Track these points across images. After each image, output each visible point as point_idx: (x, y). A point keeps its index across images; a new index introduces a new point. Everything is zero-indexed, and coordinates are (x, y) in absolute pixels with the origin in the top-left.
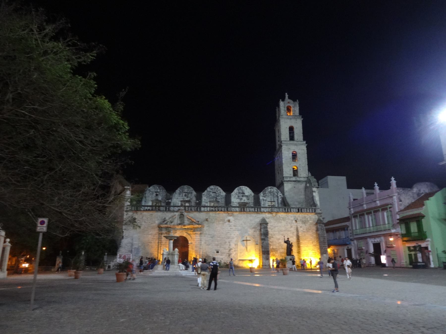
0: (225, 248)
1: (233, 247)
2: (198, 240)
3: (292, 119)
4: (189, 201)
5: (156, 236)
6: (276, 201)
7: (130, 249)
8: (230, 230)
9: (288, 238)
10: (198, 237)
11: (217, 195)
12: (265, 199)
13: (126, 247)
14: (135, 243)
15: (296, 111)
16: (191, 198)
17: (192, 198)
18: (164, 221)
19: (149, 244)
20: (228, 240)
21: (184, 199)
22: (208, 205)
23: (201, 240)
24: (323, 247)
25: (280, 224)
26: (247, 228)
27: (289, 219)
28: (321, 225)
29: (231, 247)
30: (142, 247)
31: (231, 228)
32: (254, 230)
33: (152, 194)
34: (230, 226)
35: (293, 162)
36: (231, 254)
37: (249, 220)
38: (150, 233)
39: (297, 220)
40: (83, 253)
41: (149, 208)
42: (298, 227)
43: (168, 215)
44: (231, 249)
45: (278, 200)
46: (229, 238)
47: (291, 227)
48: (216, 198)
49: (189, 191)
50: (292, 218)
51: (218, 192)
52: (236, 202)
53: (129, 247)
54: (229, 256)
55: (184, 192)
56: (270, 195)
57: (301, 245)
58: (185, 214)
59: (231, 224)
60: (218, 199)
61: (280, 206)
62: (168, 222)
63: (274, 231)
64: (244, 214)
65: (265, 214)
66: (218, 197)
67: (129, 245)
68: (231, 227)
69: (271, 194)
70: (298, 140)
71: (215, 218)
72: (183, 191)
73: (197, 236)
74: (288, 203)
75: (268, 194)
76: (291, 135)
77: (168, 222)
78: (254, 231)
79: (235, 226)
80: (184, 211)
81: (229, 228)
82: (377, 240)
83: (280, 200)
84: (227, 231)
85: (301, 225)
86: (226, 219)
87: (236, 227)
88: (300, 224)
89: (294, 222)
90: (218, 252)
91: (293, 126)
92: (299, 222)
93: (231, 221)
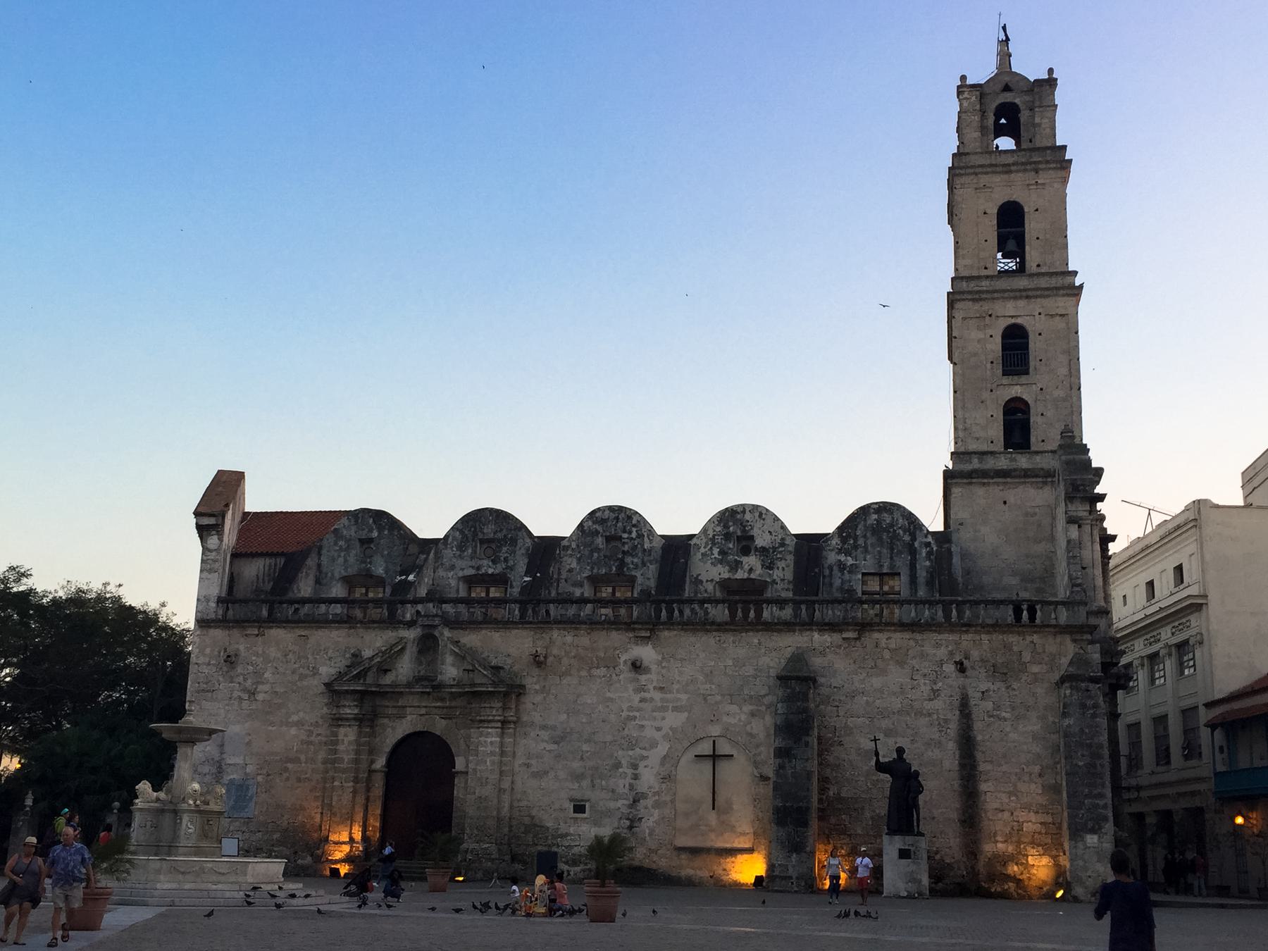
1: (650, 787)
2: (492, 753)
4: (501, 580)
5: (320, 731)
9: (900, 751)
10: (493, 739)
11: (626, 548)
12: (850, 561)
14: (230, 762)
15: (1039, 125)
16: (510, 564)
17: (514, 565)
19: (290, 766)
20: (631, 753)
21: (478, 568)
22: (583, 593)
23: (503, 753)
25: (877, 682)
26: (719, 698)
27: (923, 656)
29: (642, 786)
30: (260, 778)
32: (751, 707)
33: (348, 549)
34: (642, 689)
35: (1005, 380)
37: (730, 663)
38: (295, 718)
39: (966, 662)
40: (29, 802)
41: (337, 609)
42: (970, 692)
47: (935, 694)
48: (622, 564)
49: (504, 532)
50: (942, 653)
51: (630, 533)
52: (712, 580)
55: (480, 536)
57: (983, 787)
58: (442, 634)
60: (631, 566)
61: (922, 593)
62: (369, 669)
65: (808, 633)
66: (628, 559)
67: (206, 769)
69: (880, 540)
70: (1043, 270)
72: (475, 534)
75: (865, 536)
77: (369, 669)
78: (753, 714)
81: (637, 698)
83: (924, 564)
84: (624, 714)
85: (983, 687)
87: (668, 696)
88: (979, 683)
89: (950, 668)
90: (579, 809)
91: (1017, 200)
92: (973, 668)
93: (646, 663)
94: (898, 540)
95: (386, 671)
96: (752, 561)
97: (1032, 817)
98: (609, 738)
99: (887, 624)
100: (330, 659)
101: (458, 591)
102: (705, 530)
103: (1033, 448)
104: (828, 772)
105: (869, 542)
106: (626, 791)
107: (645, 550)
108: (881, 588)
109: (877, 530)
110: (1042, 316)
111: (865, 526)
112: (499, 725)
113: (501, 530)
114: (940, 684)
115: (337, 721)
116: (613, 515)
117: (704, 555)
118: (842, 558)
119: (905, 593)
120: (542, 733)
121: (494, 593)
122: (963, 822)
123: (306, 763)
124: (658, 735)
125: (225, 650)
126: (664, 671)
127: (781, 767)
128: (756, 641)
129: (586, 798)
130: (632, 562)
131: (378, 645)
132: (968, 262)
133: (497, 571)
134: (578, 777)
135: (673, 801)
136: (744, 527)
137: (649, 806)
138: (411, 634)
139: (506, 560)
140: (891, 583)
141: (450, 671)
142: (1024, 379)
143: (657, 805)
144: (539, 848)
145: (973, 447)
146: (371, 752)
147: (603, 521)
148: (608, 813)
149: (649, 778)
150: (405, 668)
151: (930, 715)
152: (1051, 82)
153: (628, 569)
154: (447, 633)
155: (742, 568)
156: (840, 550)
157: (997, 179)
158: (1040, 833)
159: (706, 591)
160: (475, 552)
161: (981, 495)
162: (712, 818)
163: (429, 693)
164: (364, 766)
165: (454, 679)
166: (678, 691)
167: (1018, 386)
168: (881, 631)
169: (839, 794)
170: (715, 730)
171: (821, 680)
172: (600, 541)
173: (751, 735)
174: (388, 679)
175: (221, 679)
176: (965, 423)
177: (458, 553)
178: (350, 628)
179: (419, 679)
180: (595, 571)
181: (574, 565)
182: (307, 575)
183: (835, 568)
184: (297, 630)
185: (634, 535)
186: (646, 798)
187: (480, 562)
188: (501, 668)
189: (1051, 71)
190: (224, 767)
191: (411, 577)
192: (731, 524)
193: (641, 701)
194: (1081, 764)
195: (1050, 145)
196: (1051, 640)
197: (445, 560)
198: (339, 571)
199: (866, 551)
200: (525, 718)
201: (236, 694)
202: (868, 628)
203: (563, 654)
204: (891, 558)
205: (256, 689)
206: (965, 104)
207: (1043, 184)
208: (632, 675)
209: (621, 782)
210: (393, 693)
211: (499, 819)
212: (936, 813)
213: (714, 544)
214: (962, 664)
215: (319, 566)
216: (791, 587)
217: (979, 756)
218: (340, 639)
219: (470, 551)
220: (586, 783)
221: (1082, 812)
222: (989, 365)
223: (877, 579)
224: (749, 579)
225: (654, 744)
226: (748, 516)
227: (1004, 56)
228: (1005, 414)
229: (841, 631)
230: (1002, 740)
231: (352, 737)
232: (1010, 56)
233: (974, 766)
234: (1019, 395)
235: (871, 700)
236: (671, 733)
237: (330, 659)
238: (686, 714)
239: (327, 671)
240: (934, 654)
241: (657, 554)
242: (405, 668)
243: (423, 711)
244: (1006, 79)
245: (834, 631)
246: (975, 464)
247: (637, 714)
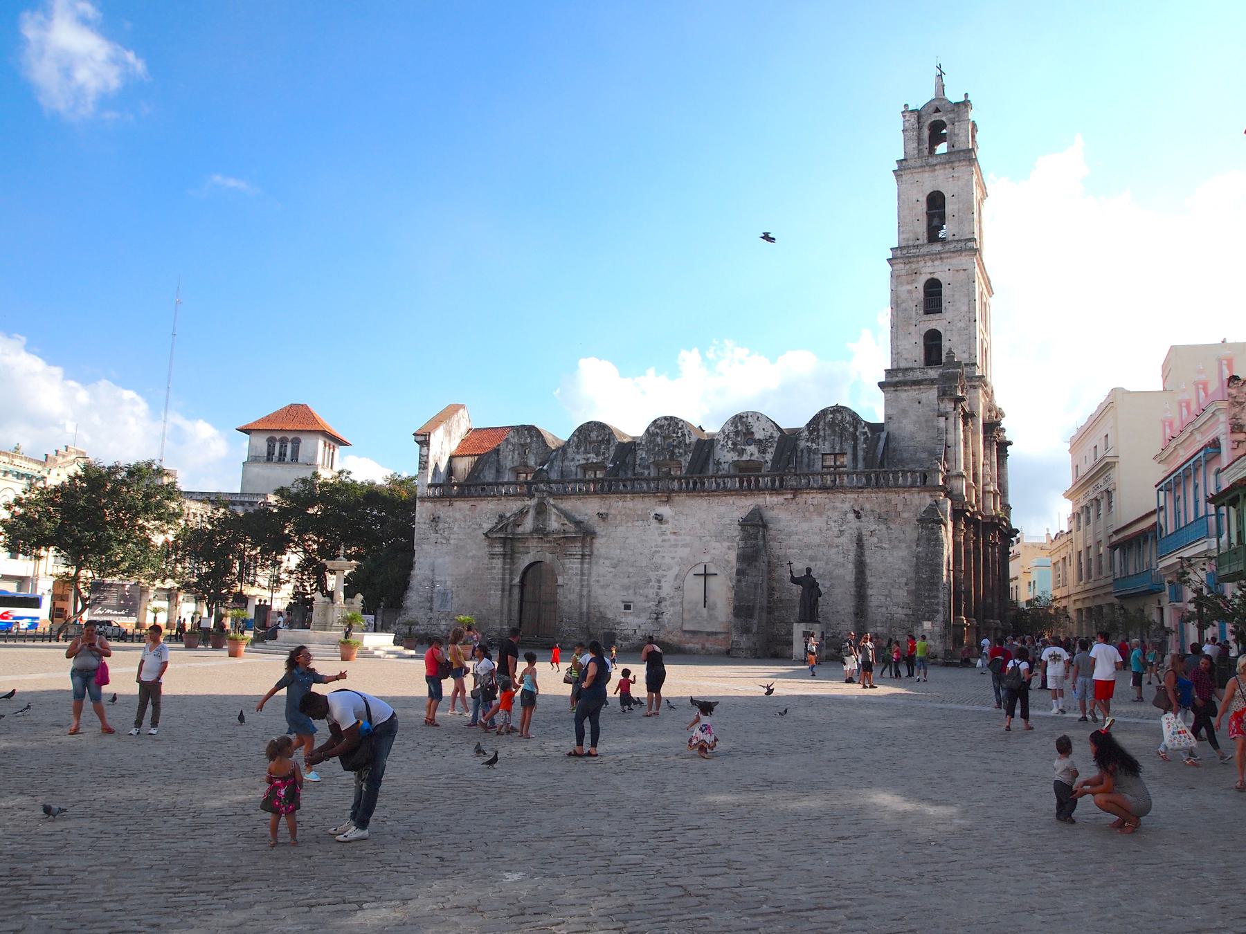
2: (577, 574)
3: (937, 167)
6: (849, 451)
7: (429, 595)
9: (809, 570)
12: (814, 446)
15: (958, 135)
20: (657, 573)
21: (588, 459)
23: (582, 574)
24: (926, 597)
25: (805, 526)
26: (708, 538)
27: (834, 508)
29: (663, 594)
31: (663, 541)
32: (730, 544)
34: (663, 533)
38: (471, 554)
44: (664, 599)
45: (855, 448)
47: (842, 532)
48: (673, 453)
49: (603, 436)
50: (847, 506)
51: (678, 433)
54: (657, 618)
57: (870, 592)
58: (549, 502)
59: (664, 527)
66: (677, 451)
69: (834, 431)
70: (956, 238)
72: (586, 438)
73: (574, 563)
75: (824, 429)
79: (675, 533)
83: (862, 446)
84: (653, 549)
86: (653, 514)
87: (679, 538)
88: (869, 524)
89: (851, 516)
90: (627, 607)
94: (846, 431)
95: (518, 526)
96: (752, 449)
97: (900, 611)
98: (644, 564)
99: (812, 488)
100: (488, 518)
101: (576, 474)
102: (723, 431)
104: (774, 584)
106: (654, 596)
108: (835, 463)
109: (832, 424)
112: (580, 557)
114: (844, 527)
115: (493, 556)
116: (667, 422)
117: (723, 446)
118: (809, 444)
122: (856, 614)
126: (676, 522)
127: (739, 581)
128: (731, 502)
132: (905, 236)
134: (627, 588)
135: (682, 603)
138: (533, 502)
139: (604, 454)
140: (842, 460)
141: (554, 524)
143: (672, 605)
144: (606, 630)
145: (903, 365)
146: (511, 574)
147: (661, 427)
148: (644, 610)
149: (667, 589)
150: (528, 524)
151: (837, 546)
152: (966, 104)
154: (552, 501)
157: (926, 175)
158: (904, 621)
160: (585, 449)
161: (907, 395)
162: (705, 612)
163: (542, 538)
164: (507, 581)
168: (807, 493)
170: (706, 559)
171: (771, 526)
172: (659, 439)
173: (728, 562)
174: (520, 530)
176: (898, 348)
179: (536, 530)
187: (589, 456)
188: (582, 522)
189: (966, 95)
191: (545, 467)
195: (965, 148)
196: (916, 495)
198: (509, 464)
200: (596, 552)
202: (800, 491)
204: (841, 443)
206: (907, 124)
207: (959, 177)
208: (658, 525)
209: (651, 591)
210: (523, 538)
211: (581, 614)
212: (839, 608)
213: (728, 438)
215: (498, 461)
217: (868, 573)
220: (631, 591)
222: (914, 308)
223: (832, 457)
224: (750, 460)
225: (670, 568)
226: (750, 419)
227: (941, 88)
229: (783, 494)
230: (883, 562)
231: (500, 566)
232: (943, 86)
235: (801, 537)
237: (488, 518)
239: (487, 526)
241: (692, 447)
242: (528, 524)
243: (539, 549)
244: (938, 104)
246: (900, 377)
247: (660, 549)
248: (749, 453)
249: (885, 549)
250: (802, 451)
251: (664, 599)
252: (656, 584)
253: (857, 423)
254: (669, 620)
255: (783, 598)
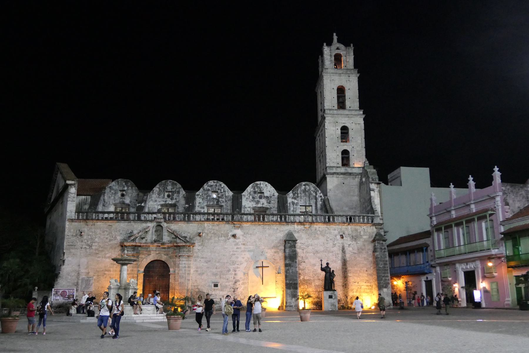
0: (228, 279)
3: (342, 75)
4: (174, 206)
8: (236, 251)
9: (328, 264)
10: (185, 262)
11: (220, 195)
12: (296, 201)
13: (70, 277)
16: (178, 200)
17: (179, 201)
18: (130, 237)
19: (106, 272)
22: (204, 211)
24: (383, 277)
25: (316, 242)
27: (330, 233)
28: (381, 242)
29: (238, 277)
31: (237, 248)
33: (116, 193)
35: (342, 144)
36: (237, 288)
37: (267, 235)
39: (344, 235)
41: (112, 215)
42: (345, 245)
43: (137, 227)
44: (238, 281)
46: (234, 263)
47: (334, 245)
48: (218, 201)
50: (336, 232)
51: (221, 190)
52: (250, 207)
53: (74, 277)
54: (234, 291)
56: (303, 196)
57: (349, 275)
59: (237, 241)
60: (221, 202)
61: (319, 212)
62: (137, 238)
63: (307, 252)
64: (260, 225)
65: (293, 225)
66: (220, 199)
68: (239, 246)
69: (305, 194)
70: (351, 109)
71: (212, 232)
72: (164, 190)
73: (183, 260)
74: (331, 209)
75: (301, 193)
76: (341, 100)
79: (244, 244)
80: (162, 220)
81: (235, 247)
82: (470, 266)
83: (320, 203)
84: (231, 253)
86: (231, 234)
87: (246, 247)
88: (347, 241)
89: (339, 237)
91: (344, 86)
93: (237, 236)
94: (311, 195)
96: (263, 201)
97: (364, 284)
98: (226, 261)
103: (351, 166)
105: (302, 195)
107: (226, 197)
110: (353, 124)
111: (301, 190)
113: (174, 188)
117: (247, 198)
119: (314, 212)
120: (202, 260)
121: (171, 210)
123: (113, 271)
124: (243, 260)
125: (79, 230)
126: (245, 238)
128: (276, 228)
129: (218, 282)
130: (222, 200)
131: (139, 229)
133: (173, 203)
134: (215, 275)
136: (261, 189)
137: (241, 284)
141: (166, 238)
142: (347, 144)
148: (226, 287)
151: (332, 252)
153: (220, 203)
155: (260, 203)
156: (293, 197)
159: (248, 211)
163: (159, 246)
165: (169, 241)
166: (250, 245)
167: (346, 146)
169: (304, 278)
175: (78, 241)
177: (158, 196)
178: (129, 222)
180: (208, 203)
181: (201, 201)
182: (101, 203)
183: (291, 204)
184: (107, 223)
185: (222, 191)
186: (240, 282)
188: (186, 237)
190: (80, 273)
191: (143, 204)
192: (256, 188)
193: (237, 249)
194: (381, 267)
197: (153, 199)
199: (301, 198)
201: (84, 246)
203: (209, 232)
204: (309, 201)
205: (92, 244)
209: (231, 276)
213: (250, 195)
214: (342, 235)
216: (277, 209)
217: (348, 265)
218: (125, 227)
219: (162, 195)
221: (382, 281)
223: (304, 207)
228: (342, 154)
233: (346, 269)
234: (346, 149)
235: (314, 247)
236: (247, 259)
238: (253, 253)
240: (334, 233)
242: (151, 236)
243: (158, 252)
245: (302, 225)
248: (262, 203)
249: (356, 253)
250: (290, 204)
251: (238, 281)
252: (233, 273)
253: (317, 191)
254: (241, 293)
255: (305, 279)
